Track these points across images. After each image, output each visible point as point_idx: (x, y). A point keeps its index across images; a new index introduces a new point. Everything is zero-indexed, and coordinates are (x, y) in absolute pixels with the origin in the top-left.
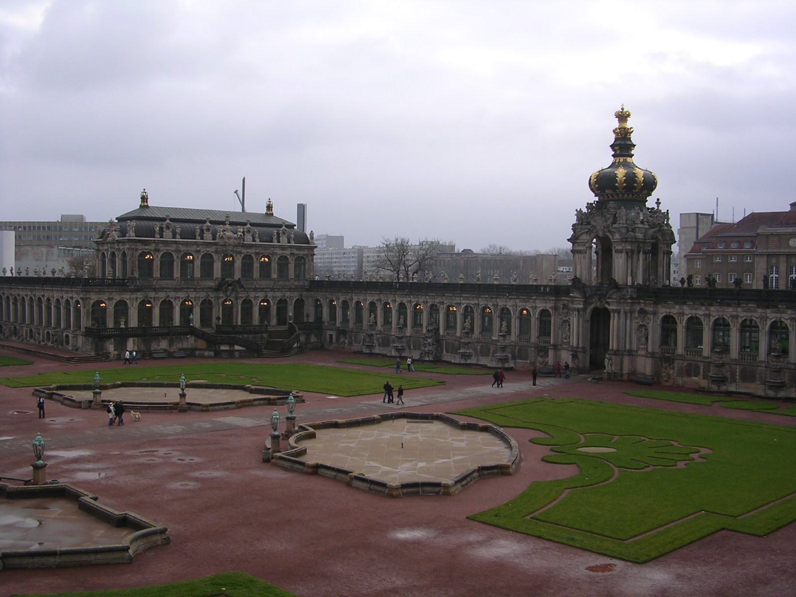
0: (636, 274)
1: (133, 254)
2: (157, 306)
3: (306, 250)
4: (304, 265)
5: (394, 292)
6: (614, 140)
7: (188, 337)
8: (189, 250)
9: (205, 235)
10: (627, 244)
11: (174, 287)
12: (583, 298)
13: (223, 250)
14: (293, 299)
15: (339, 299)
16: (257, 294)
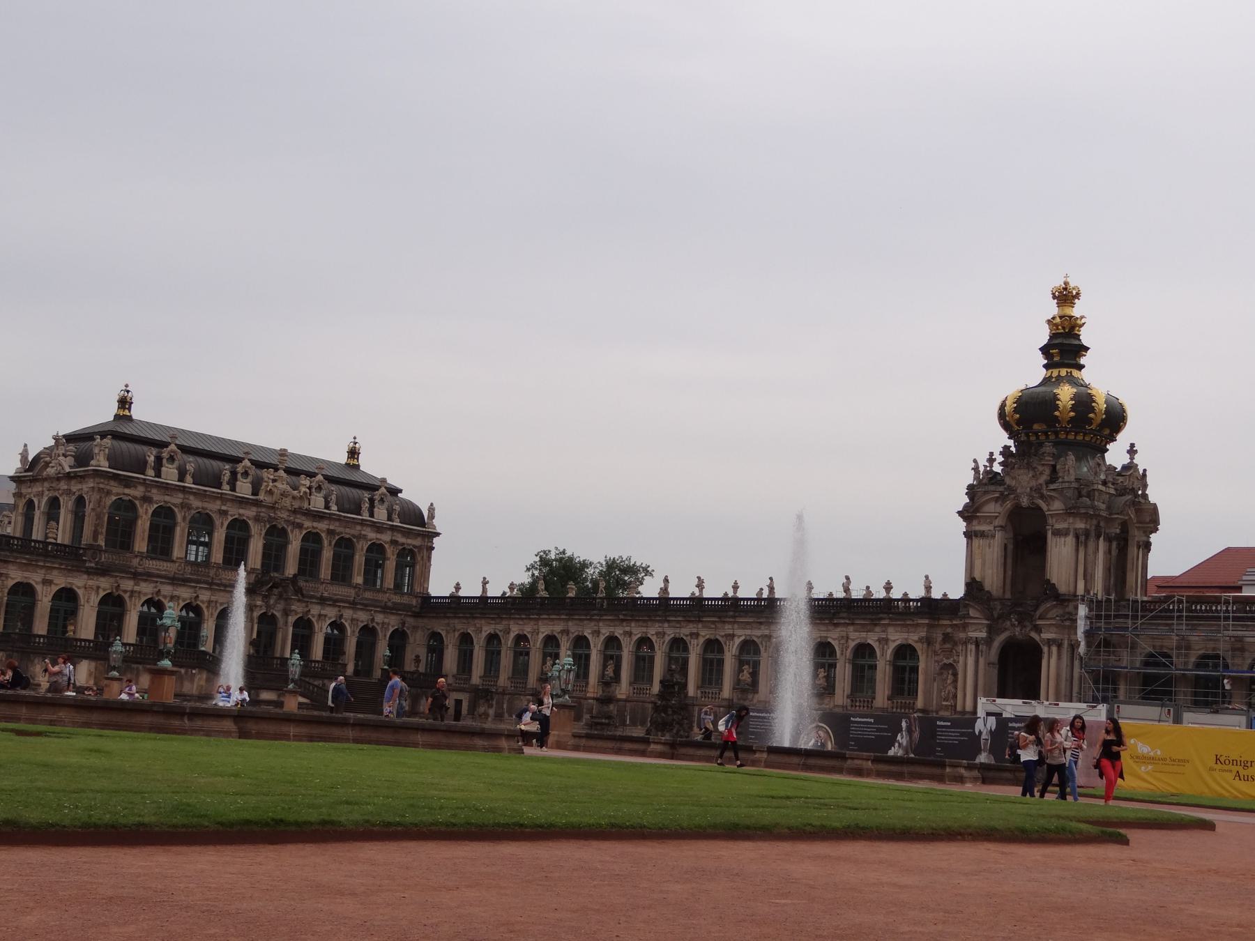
0: (1093, 576)
1: (99, 501)
2: (134, 609)
3: (419, 539)
4: (412, 566)
5: (598, 615)
6: (1049, 338)
7: (194, 671)
8: (206, 509)
9: (238, 482)
10: (1078, 520)
11: (171, 575)
12: (988, 620)
13: (269, 515)
14: (387, 629)
15: (481, 631)
16: (324, 610)
